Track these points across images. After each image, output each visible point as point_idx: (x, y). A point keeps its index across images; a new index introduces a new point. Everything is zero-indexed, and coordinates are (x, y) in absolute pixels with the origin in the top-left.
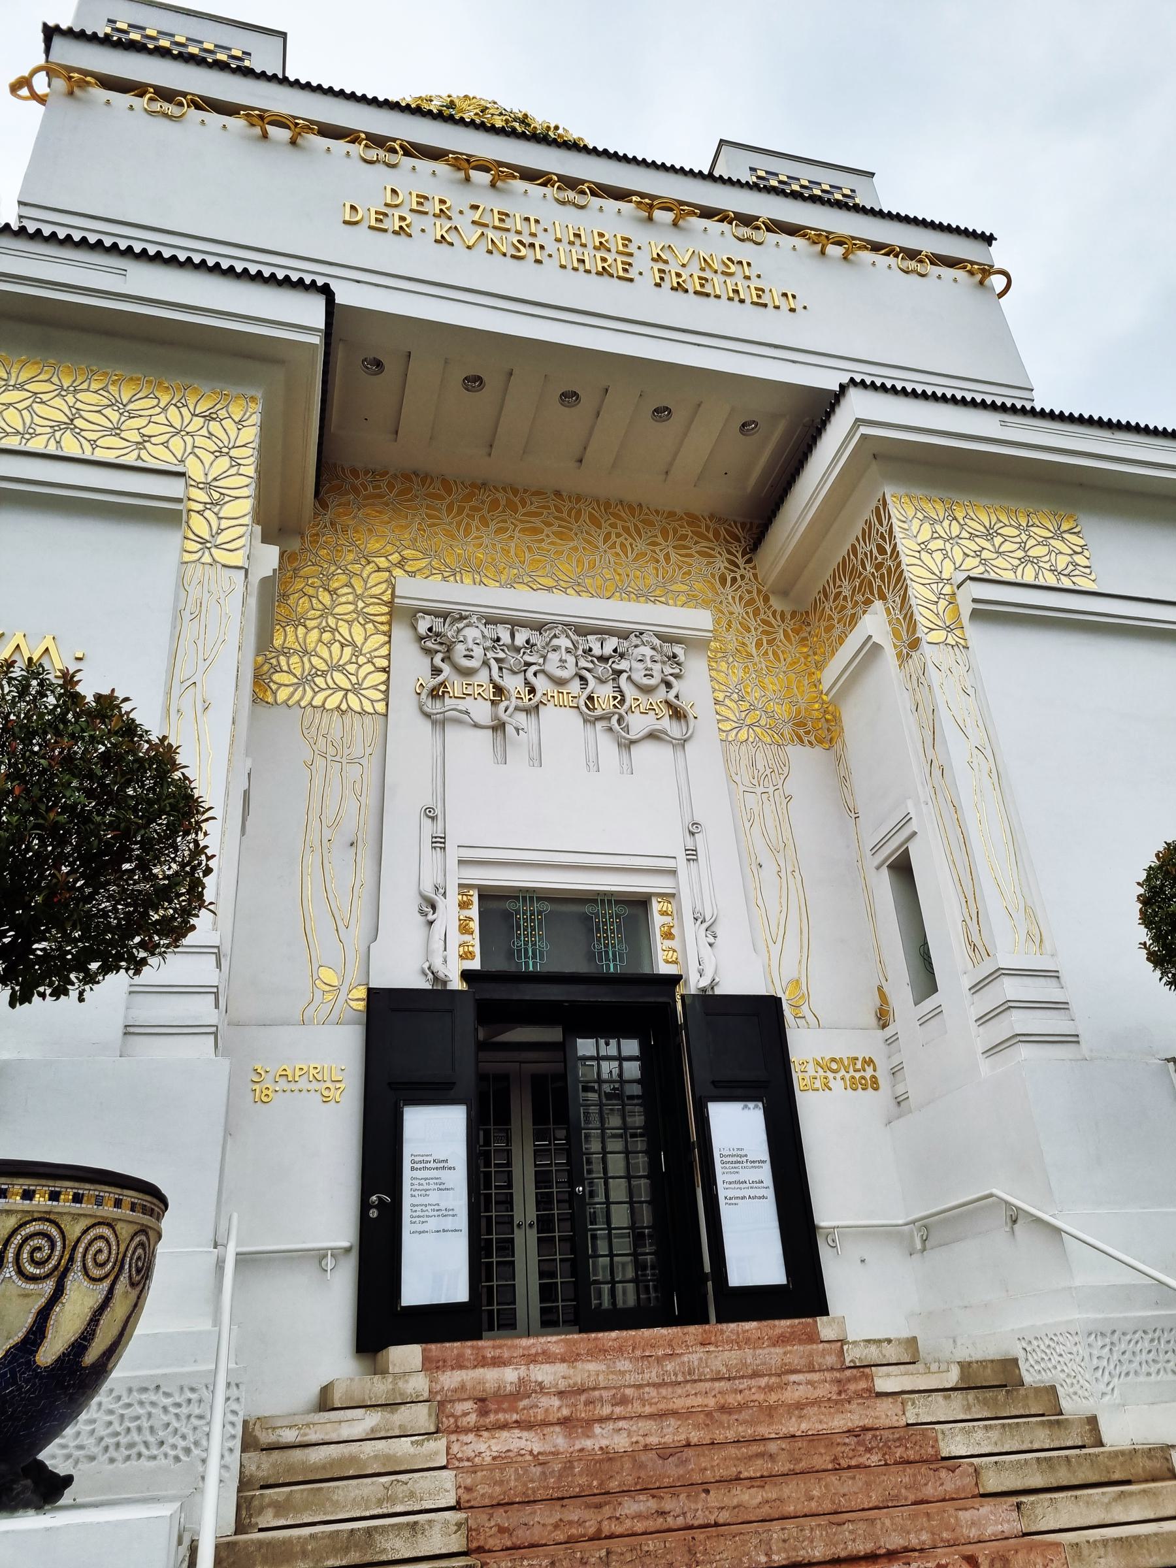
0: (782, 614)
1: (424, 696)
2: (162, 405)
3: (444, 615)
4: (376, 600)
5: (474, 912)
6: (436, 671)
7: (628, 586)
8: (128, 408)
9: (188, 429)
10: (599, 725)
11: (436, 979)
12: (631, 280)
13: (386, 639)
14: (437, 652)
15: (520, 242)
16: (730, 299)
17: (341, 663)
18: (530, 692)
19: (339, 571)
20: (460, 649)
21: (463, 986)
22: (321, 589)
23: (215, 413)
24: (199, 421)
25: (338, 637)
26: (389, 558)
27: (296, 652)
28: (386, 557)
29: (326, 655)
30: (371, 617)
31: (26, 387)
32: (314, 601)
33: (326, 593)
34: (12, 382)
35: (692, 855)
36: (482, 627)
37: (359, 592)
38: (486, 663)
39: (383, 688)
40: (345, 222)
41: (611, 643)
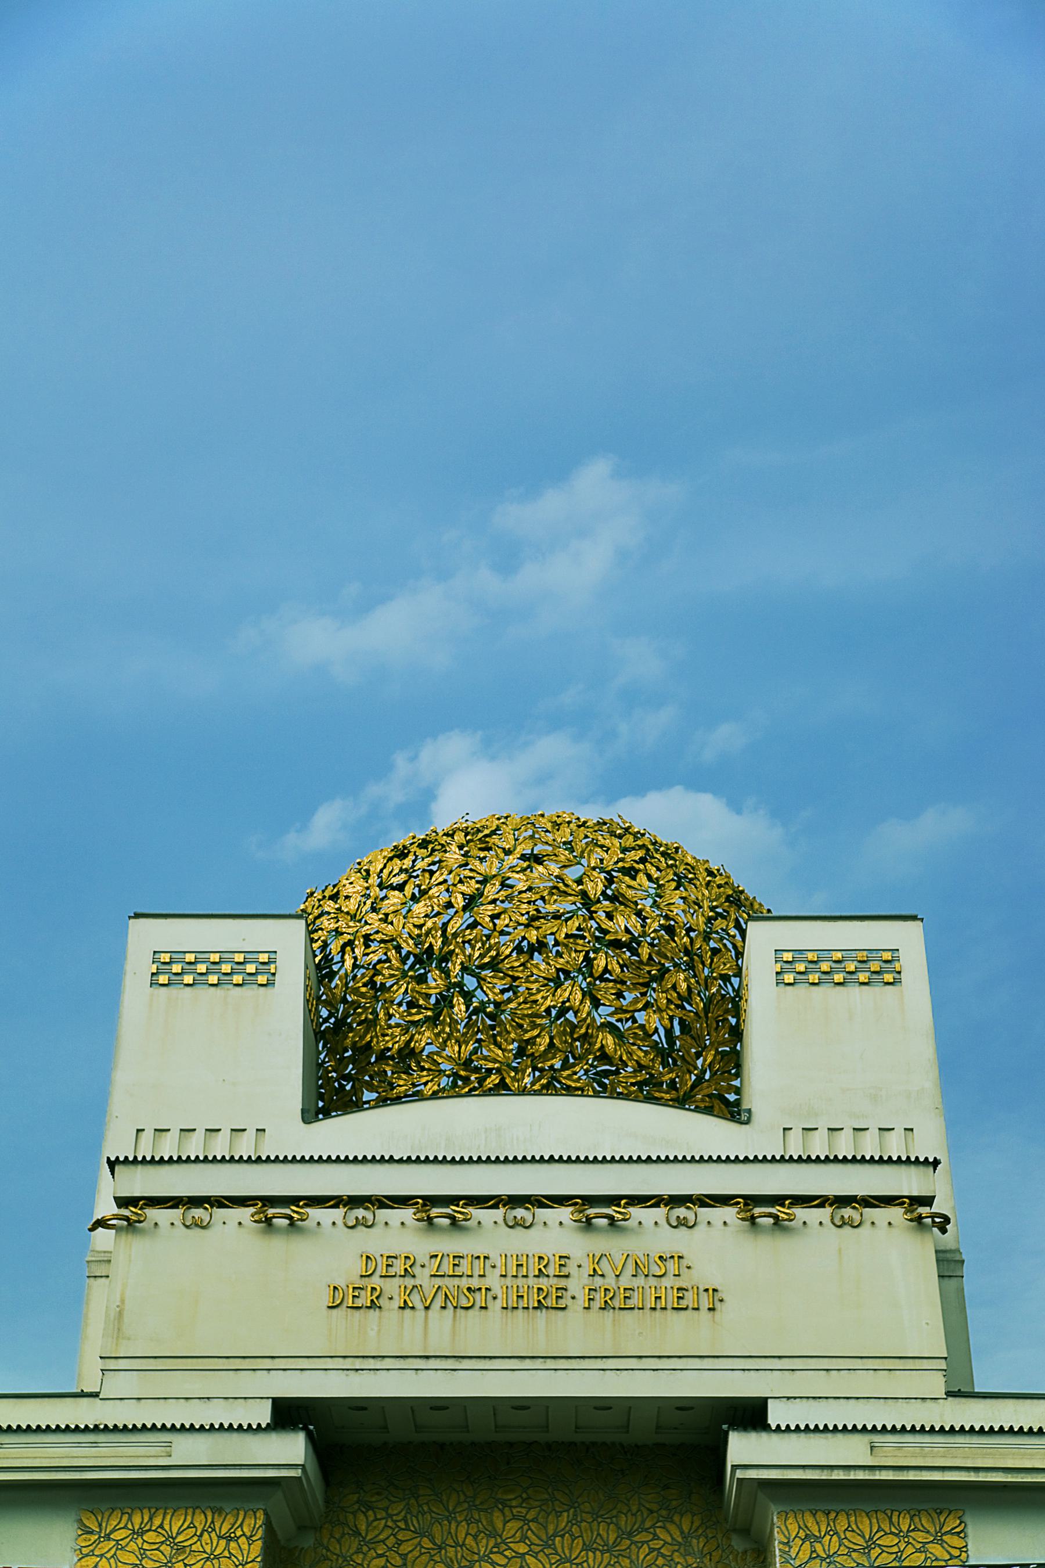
0: (745, 1552)
2: (198, 1534)
7: (595, 1542)
8: (176, 1541)
9: (215, 1554)
12: (564, 1309)
15: (469, 1289)
16: (654, 1309)
19: (345, 1563)
23: (234, 1532)
24: (223, 1542)
26: (387, 1542)
31: (112, 1536)
34: (102, 1535)
40: (330, 1307)
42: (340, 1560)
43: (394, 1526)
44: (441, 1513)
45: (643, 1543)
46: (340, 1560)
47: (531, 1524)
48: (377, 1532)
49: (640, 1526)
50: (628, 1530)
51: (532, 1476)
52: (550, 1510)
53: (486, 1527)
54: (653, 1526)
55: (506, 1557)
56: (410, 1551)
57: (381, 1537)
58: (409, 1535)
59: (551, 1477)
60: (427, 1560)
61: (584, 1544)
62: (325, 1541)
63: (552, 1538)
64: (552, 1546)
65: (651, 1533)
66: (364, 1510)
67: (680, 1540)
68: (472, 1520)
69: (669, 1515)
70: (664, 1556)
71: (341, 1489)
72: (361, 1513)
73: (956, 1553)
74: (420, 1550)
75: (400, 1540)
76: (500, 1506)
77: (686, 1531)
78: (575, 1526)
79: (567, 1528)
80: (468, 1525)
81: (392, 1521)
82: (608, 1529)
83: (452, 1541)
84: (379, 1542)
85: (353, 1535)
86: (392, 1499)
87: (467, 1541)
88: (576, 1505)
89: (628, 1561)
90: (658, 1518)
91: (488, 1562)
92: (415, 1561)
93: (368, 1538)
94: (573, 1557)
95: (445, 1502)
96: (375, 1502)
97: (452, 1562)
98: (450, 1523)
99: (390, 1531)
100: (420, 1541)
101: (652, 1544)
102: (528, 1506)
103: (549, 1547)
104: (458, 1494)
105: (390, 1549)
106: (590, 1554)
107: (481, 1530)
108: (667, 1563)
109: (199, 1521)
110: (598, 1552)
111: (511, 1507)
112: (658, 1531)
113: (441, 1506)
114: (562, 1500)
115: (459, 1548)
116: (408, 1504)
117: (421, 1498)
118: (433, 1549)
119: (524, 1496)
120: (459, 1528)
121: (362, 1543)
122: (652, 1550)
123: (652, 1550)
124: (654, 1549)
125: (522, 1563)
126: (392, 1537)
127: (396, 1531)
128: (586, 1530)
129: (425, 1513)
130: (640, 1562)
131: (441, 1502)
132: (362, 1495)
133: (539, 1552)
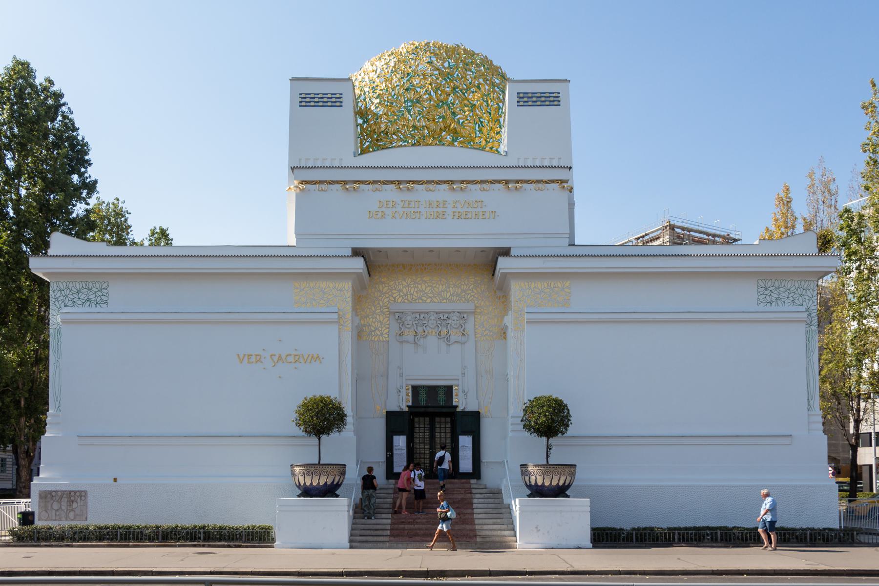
5: (410, 391)
6: (400, 329)
10: (442, 340)
11: (400, 408)
18: (424, 332)
20: (406, 322)
21: (407, 409)
24: (339, 292)
27: (367, 326)
28: (388, 293)
29: (374, 326)
35: (463, 375)
36: (411, 315)
37: (381, 305)
38: (413, 324)
41: (446, 315)
54: (472, 289)
58: (396, 292)
70: (475, 298)
73: (568, 294)
103: (439, 295)
105: (390, 296)
109: (331, 285)
111: (428, 283)
112: (474, 290)
122: (471, 296)
123: (471, 296)
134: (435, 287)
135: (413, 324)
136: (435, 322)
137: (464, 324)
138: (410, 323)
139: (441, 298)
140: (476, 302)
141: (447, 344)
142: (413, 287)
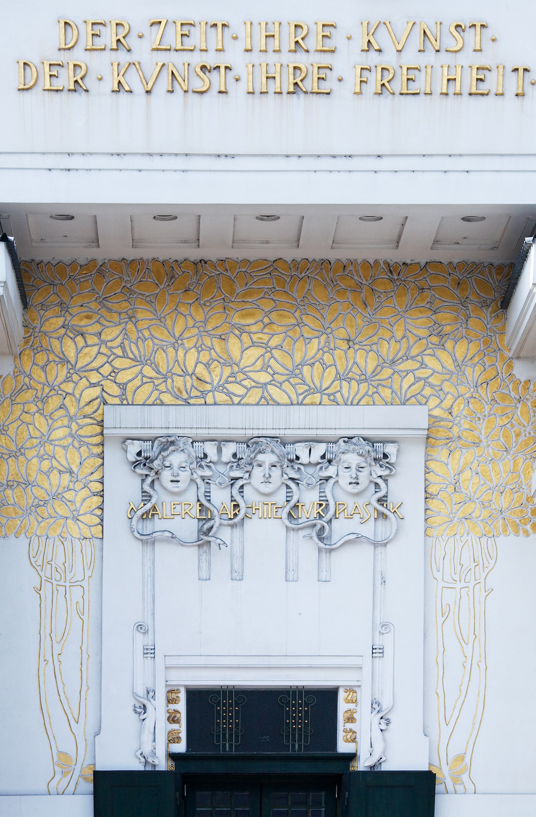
1: (135, 519)
3: (153, 440)
4: (89, 421)
13: (101, 460)
14: (147, 475)
17: (59, 491)
19: (53, 392)
20: (166, 475)
21: (171, 763)
22: (37, 415)
25: (55, 464)
26: (100, 370)
28: (97, 370)
29: (46, 485)
30: (86, 440)
32: (31, 427)
33: (43, 420)
37: (72, 411)
39: (99, 512)
42: (47, 390)
43: (109, 353)
44: (165, 339)
45: (408, 372)
46: (47, 390)
47: (274, 351)
48: (88, 359)
49: (406, 352)
50: (391, 358)
51: (275, 298)
52: (298, 336)
53: (221, 355)
55: (244, 386)
56: (130, 381)
57: (95, 365)
58: (126, 363)
59: (299, 300)
60: (151, 390)
61: (338, 373)
62: (27, 369)
63: (300, 367)
64: (300, 376)
65: (419, 362)
66: (72, 335)
67: (452, 368)
68: (203, 346)
69: (440, 342)
70: (431, 386)
71: (42, 312)
72: (68, 338)
74: (142, 380)
75: (117, 369)
76: (237, 332)
77: (460, 358)
78: (326, 354)
79: (318, 356)
80: (199, 352)
81: (106, 347)
82: (366, 357)
83: (180, 369)
84: (91, 370)
85: (60, 362)
86: (105, 323)
87: (197, 371)
88: (329, 331)
89: (390, 391)
90: (428, 345)
91: (224, 393)
92: (136, 391)
93: (79, 365)
94: (323, 388)
95: (170, 327)
96: (85, 326)
97: (181, 392)
98: (177, 351)
99: (105, 359)
100: (142, 370)
101: (418, 374)
102: (271, 332)
103: (296, 376)
104: (185, 318)
106: (345, 384)
107: (214, 358)
108: (435, 393)
110: (353, 381)
111: (249, 333)
113: (166, 332)
114: (312, 325)
115: (188, 378)
116: (124, 329)
117: (140, 322)
118: (158, 379)
119: (266, 320)
120: (187, 355)
121: (72, 371)
122: (417, 379)
123: (417, 379)
124: (421, 379)
125: (263, 393)
126: (107, 365)
127: (112, 358)
128: (340, 358)
129: (146, 340)
130: (403, 392)
131: (165, 327)
132: (69, 319)
133: (284, 381)
134: (279, 347)
135: (192, 480)
136: (276, 473)
137: (386, 481)
138: (184, 476)
139: (302, 389)
140: (433, 402)
141: (320, 550)
142: (195, 346)
